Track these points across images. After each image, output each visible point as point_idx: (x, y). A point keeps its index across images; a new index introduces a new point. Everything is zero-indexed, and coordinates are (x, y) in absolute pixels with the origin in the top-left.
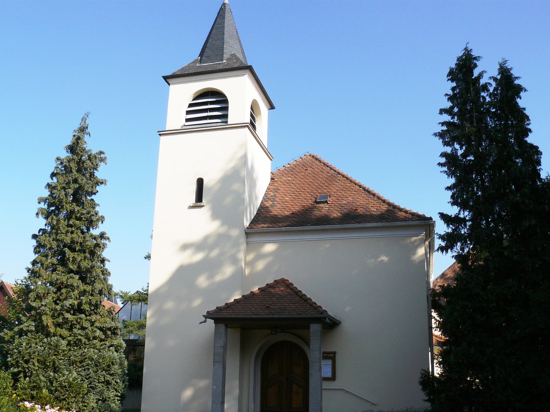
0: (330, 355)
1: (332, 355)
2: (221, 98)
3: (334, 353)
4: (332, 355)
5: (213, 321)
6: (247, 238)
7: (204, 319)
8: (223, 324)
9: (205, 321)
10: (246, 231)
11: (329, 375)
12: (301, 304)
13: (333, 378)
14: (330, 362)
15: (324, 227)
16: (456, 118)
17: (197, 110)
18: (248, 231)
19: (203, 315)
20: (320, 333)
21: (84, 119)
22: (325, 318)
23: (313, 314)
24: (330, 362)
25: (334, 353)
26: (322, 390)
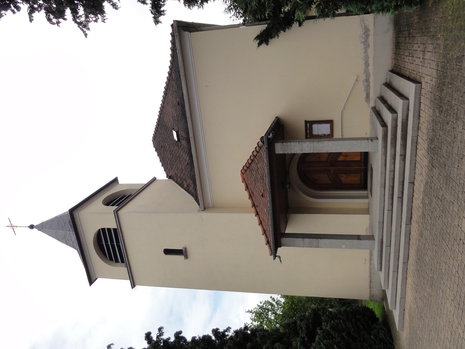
0: (308, 127)
1: (308, 124)
2: (101, 232)
3: (306, 122)
4: (308, 124)
5: (279, 248)
6: (208, 208)
7: (277, 258)
8: (281, 239)
9: (279, 257)
10: (203, 210)
11: (328, 126)
12: (258, 162)
13: (331, 122)
14: (315, 126)
15: (182, 76)
16: (54, 7)
17: (115, 250)
18: (202, 208)
19: (274, 260)
20: (284, 143)
21: (6, 226)
22: (268, 139)
23: (264, 155)
24: (315, 126)
25: (306, 122)
26: (343, 139)
